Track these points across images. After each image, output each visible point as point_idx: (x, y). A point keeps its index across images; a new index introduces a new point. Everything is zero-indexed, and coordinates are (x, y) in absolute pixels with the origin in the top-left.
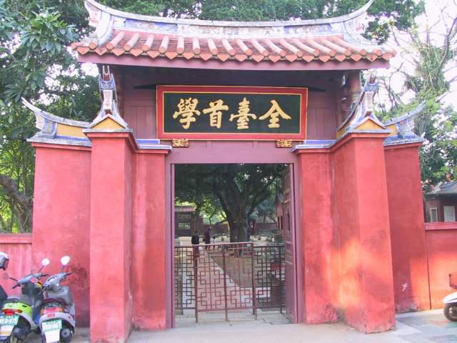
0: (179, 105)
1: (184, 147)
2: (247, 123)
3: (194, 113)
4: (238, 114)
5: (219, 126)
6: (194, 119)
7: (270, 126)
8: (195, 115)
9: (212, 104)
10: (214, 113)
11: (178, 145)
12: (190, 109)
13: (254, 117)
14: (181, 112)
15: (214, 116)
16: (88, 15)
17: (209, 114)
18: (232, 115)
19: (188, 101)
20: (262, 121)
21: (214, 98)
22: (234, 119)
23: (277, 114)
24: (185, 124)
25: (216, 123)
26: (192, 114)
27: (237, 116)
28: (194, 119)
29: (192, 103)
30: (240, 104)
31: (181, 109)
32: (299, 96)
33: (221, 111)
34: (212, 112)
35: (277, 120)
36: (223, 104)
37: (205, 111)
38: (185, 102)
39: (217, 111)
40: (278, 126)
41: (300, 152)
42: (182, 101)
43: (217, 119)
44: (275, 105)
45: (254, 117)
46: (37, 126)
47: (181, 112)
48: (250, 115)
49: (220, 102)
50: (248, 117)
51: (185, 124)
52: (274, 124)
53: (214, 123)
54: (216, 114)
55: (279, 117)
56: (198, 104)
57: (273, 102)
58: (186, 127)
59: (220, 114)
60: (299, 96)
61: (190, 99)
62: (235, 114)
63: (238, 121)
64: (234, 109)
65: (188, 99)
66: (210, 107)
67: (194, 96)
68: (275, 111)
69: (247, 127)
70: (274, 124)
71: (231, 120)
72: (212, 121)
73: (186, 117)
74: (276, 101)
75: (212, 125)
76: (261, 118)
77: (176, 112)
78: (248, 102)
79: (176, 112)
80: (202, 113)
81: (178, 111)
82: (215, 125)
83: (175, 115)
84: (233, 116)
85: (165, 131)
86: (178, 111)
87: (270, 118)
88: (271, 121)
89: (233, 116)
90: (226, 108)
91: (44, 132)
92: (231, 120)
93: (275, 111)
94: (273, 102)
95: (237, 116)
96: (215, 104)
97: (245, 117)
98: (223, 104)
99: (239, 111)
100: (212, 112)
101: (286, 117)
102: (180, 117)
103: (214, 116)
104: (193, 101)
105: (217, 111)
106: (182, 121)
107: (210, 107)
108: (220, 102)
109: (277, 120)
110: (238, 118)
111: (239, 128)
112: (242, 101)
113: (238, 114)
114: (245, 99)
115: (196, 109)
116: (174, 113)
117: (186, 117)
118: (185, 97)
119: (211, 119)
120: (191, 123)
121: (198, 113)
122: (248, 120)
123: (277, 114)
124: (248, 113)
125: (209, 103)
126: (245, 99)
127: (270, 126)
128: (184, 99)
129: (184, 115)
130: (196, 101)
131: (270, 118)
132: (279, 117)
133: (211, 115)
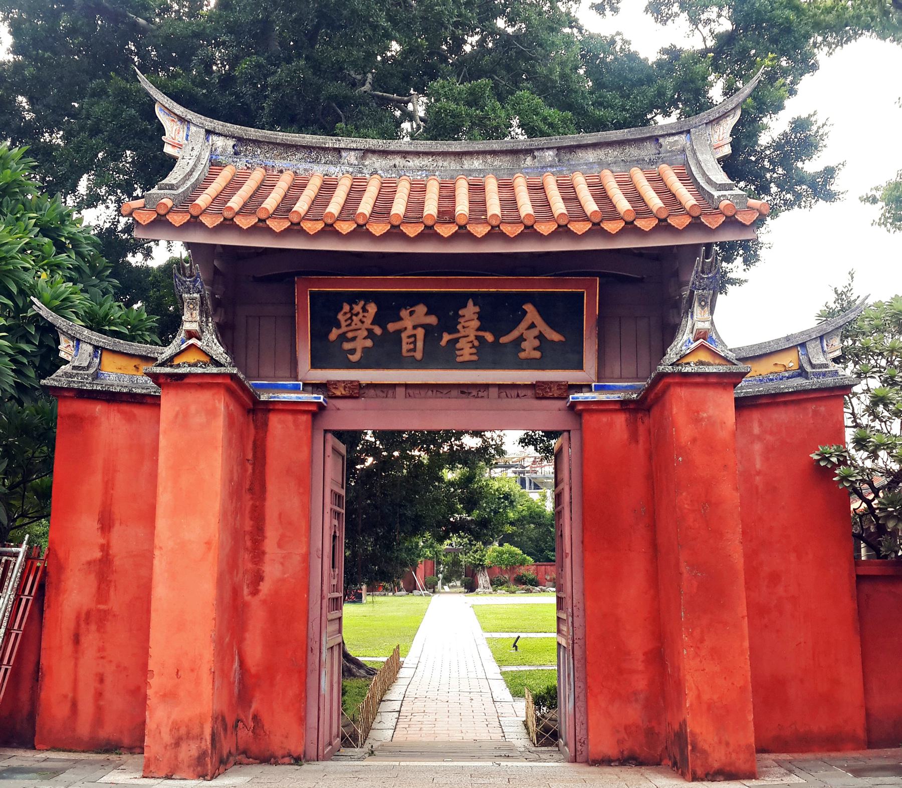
0: (340, 317)
1: (351, 397)
2: (474, 350)
3: (370, 332)
5: (419, 355)
6: (369, 343)
7: (522, 355)
8: (371, 334)
9: (404, 313)
10: (410, 331)
11: (338, 393)
12: (363, 322)
13: (489, 337)
14: (344, 329)
15: (409, 337)
16: (161, 130)
17: (399, 332)
19: (357, 308)
20: (504, 345)
21: (411, 300)
22: (448, 342)
23: (535, 332)
24: (353, 351)
25: (414, 350)
26: (365, 333)
28: (369, 343)
29: (364, 310)
30: (461, 312)
31: (343, 324)
33: (422, 326)
34: (406, 329)
35: (537, 343)
36: (427, 314)
37: (392, 327)
38: (351, 309)
39: (415, 327)
40: (537, 354)
41: (580, 407)
42: (346, 307)
43: (415, 343)
44: (531, 313)
45: (489, 337)
46: (62, 355)
47: (344, 329)
48: (481, 333)
49: (421, 309)
50: (477, 337)
51: (353, 351)
52: (529, 349)
53: (409, 351)
54: (414, 332)
55: (540, 337)
56: (376, 313)
57: (529, 307)
58: (355, 358)
59: (420, 332)
61: (362, 303)
62: (450, 333)
63: (458, 346)
64: (449, 323)
65: (357, 304)
66: (401, 319)
67: (367, 297)
68: (532, 326)
69: (475, 358)
70: (529, 349)
71: (443, 343)
72: (405, 347)
74: (535, 306)
76: (503, 340)
78: (477, 309)
79: (334, 330)
81: (339, 326)
83: (334, 334)
84: (446, 337)
85: (314, 366)
86: (339, 326)
87: (521, 339)
88: (524, 345)
89: (446, 337)
90: (432, 320)
91: (74, 368)
92: (443, 343)
93: (532, 326)
94: (529, 307)
96: (411, 313)
97: (472, 338)
98: (427, 314)
99: (459, 327)
100: (406, 329)
101: (555, 337)
102: (343, 338)
103: (409, 337)
105: (415, 327)
106: (347, 346)
107: (401, 319)
108: (421, 309)
109: (537, 343)
110: (457, 340)
111: (459, 359)
112: (465, 306)
113: (458, 331)
114: (470, 303)
115: (372, 324)
116: (331, 331)
117: (354, 339)
118: (353, 298)
120: (365, 350)
121: (378, 331)
122: (476, 343)
123: (535, 332)
124: (478, 329)
125: (399, 310)
126: (470, 303)
127: (522, 355)
128: (351, 305)
129: (350, 335)
130: (372, 309)
132: (540, 337)
133: (404, 335)
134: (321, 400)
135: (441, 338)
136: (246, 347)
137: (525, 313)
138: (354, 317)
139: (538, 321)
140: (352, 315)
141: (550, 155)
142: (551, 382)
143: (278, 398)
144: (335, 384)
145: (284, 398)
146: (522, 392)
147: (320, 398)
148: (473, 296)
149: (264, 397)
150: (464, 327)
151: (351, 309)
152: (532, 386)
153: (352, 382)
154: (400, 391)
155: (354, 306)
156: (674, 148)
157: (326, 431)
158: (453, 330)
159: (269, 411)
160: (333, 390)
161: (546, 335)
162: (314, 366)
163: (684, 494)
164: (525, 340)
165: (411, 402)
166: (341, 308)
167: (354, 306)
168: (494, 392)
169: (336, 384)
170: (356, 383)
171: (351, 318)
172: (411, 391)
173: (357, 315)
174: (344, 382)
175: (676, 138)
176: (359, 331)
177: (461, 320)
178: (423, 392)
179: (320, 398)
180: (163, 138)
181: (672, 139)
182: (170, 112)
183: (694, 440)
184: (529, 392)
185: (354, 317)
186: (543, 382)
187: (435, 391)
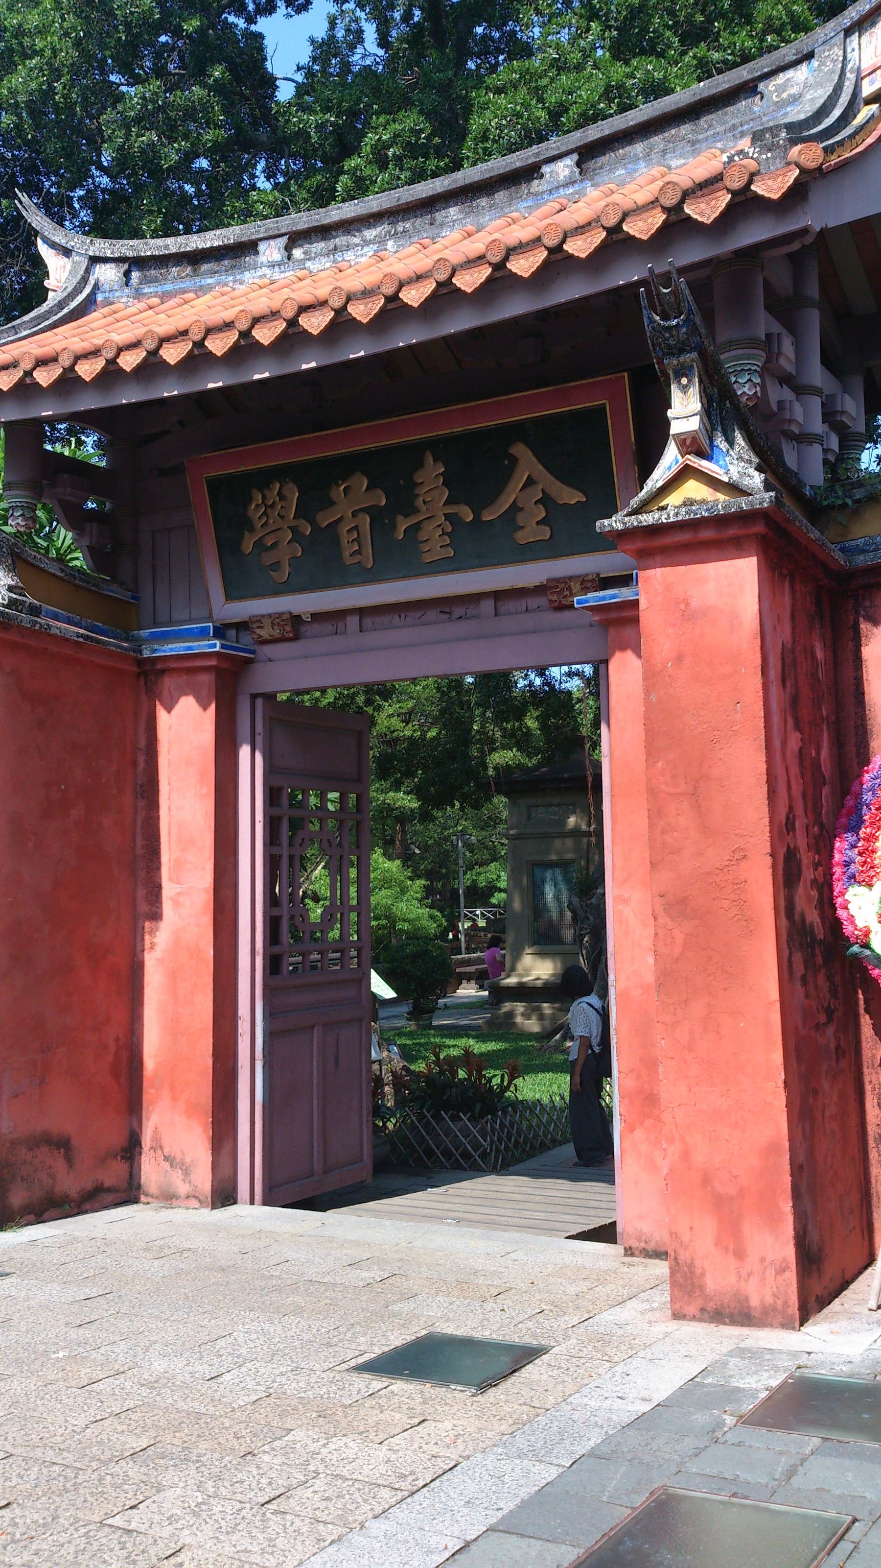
1: (282, 640)
4: (417, 511)
7: (522, 537)
11: (265, 633)
12: (282, 517)
15: (349, 531)
18: (400, 518)
24: (276, 566)
27: (413, 520)
29: (282, 498)
30: (418, 478)
32: (602, 408)
33: (363, 510)
37: (325, 519)
48: (450, 510)
55: (546, 500)
57: (520, 450)
60: (602, 408)
62: (406, 516)
63: (423, 535)
66: (332, 503)
73: (274, 545)
75: (349, 560)
76: (488, 516)
77: (247, 534)
79: (247, 534)
80: (313, 523)
81: (252, 529)
82: (357, 558)
84: (403, 525)
85: (230, 596)
86: (252, 529)
88: (520, 519)
93: (530, 482)
94: (520, 450)
95: (413, 520)
99: (419, 502)
102: (259, 544)
104: (285, 492)
106: (268, 559)
107: (332, 503)
112: (420, 465)
113: (417, 511)
114: (429, 459)
119: (344, 542)
126: (429, 459)
127: (522, 537)
128: (261, 490)
131: (515, 508)
132: (546, 500)
133: (344, 529)
134: (217, 649)
135: (394, 527)
136: (154, 578)
137: (514, 460)
138: (269, 511)
139: (539, 469)
140: (266, 507)
141: (564, 168)
142: (570, 578)
143: (164, 651)
144: (259, 621)
145: (171, 650)
146: (534, 602)
147: (215, 646)
148: (432, 445)
149: (146, 654)
150: (425, 502)
151: (264, 498)
152: (540, 590)
153: (280, 615)
154: (353, 622)
155: (267, 492)
156: (784, 95)
157: (254, 697)
158: (410, 509)
159: (163, 672)
160: (258, 631)
161: (553, 494)
162: (230, 596)
163: (660, 764)
164: (521, 509)
165: (369, 638)
166: (250, 500)
167: (267, 492)
168: (488, 606)
169: (259, 620)
170: (286, 616)
171: (264, 513)
172: (368, 621)
173: (272, 506)
174: (270, 615)
175: (790, 73)
176: (279, 533)
177: (421, 491)
178: (385, 619)
179: (215, 646)
180: (46, 283)
181: (781, 78)
182: (53, 245)
183: (679, 659)
184: (542, 601)
185: (269, 511)
186: (558, 580)
187: (403, 616)
